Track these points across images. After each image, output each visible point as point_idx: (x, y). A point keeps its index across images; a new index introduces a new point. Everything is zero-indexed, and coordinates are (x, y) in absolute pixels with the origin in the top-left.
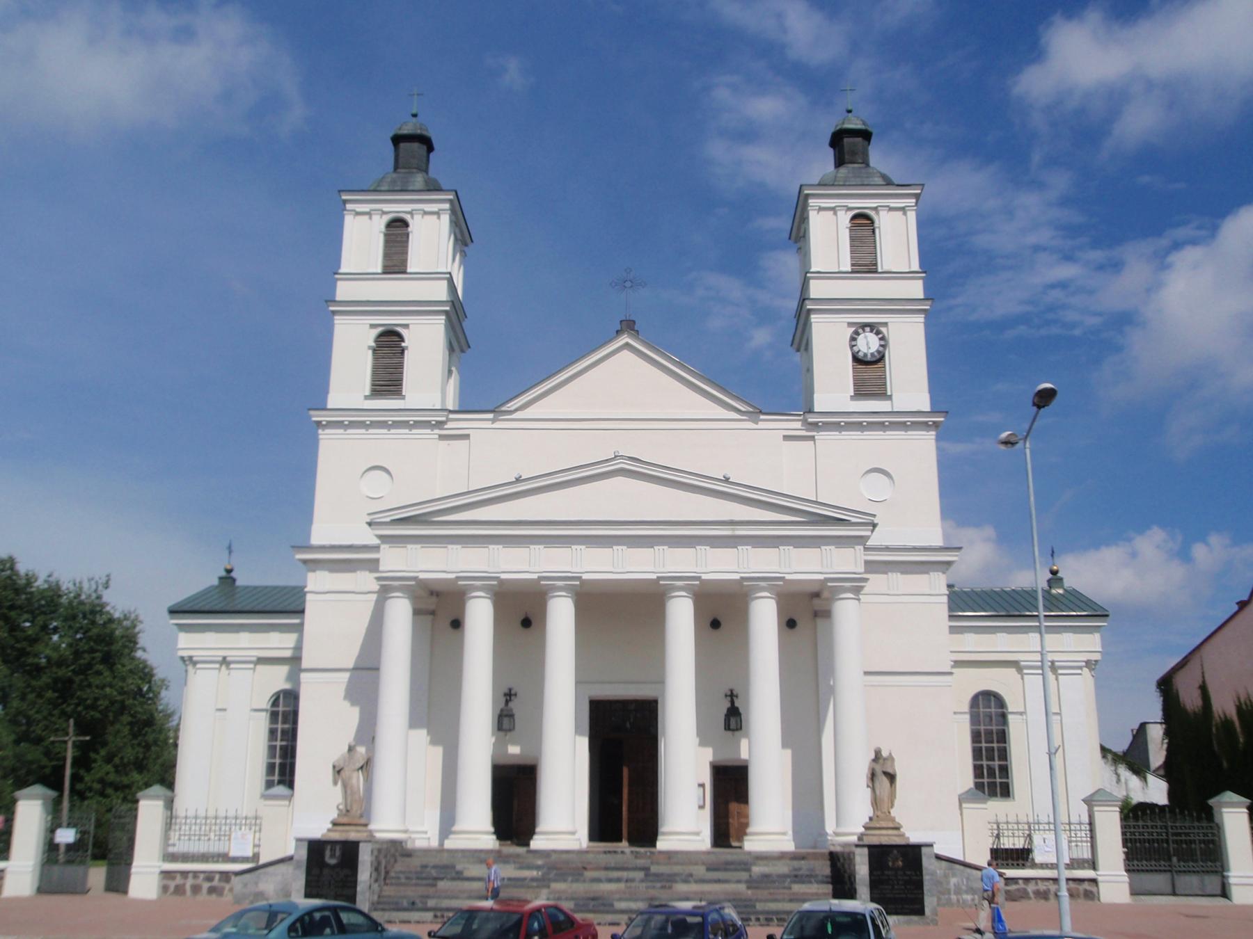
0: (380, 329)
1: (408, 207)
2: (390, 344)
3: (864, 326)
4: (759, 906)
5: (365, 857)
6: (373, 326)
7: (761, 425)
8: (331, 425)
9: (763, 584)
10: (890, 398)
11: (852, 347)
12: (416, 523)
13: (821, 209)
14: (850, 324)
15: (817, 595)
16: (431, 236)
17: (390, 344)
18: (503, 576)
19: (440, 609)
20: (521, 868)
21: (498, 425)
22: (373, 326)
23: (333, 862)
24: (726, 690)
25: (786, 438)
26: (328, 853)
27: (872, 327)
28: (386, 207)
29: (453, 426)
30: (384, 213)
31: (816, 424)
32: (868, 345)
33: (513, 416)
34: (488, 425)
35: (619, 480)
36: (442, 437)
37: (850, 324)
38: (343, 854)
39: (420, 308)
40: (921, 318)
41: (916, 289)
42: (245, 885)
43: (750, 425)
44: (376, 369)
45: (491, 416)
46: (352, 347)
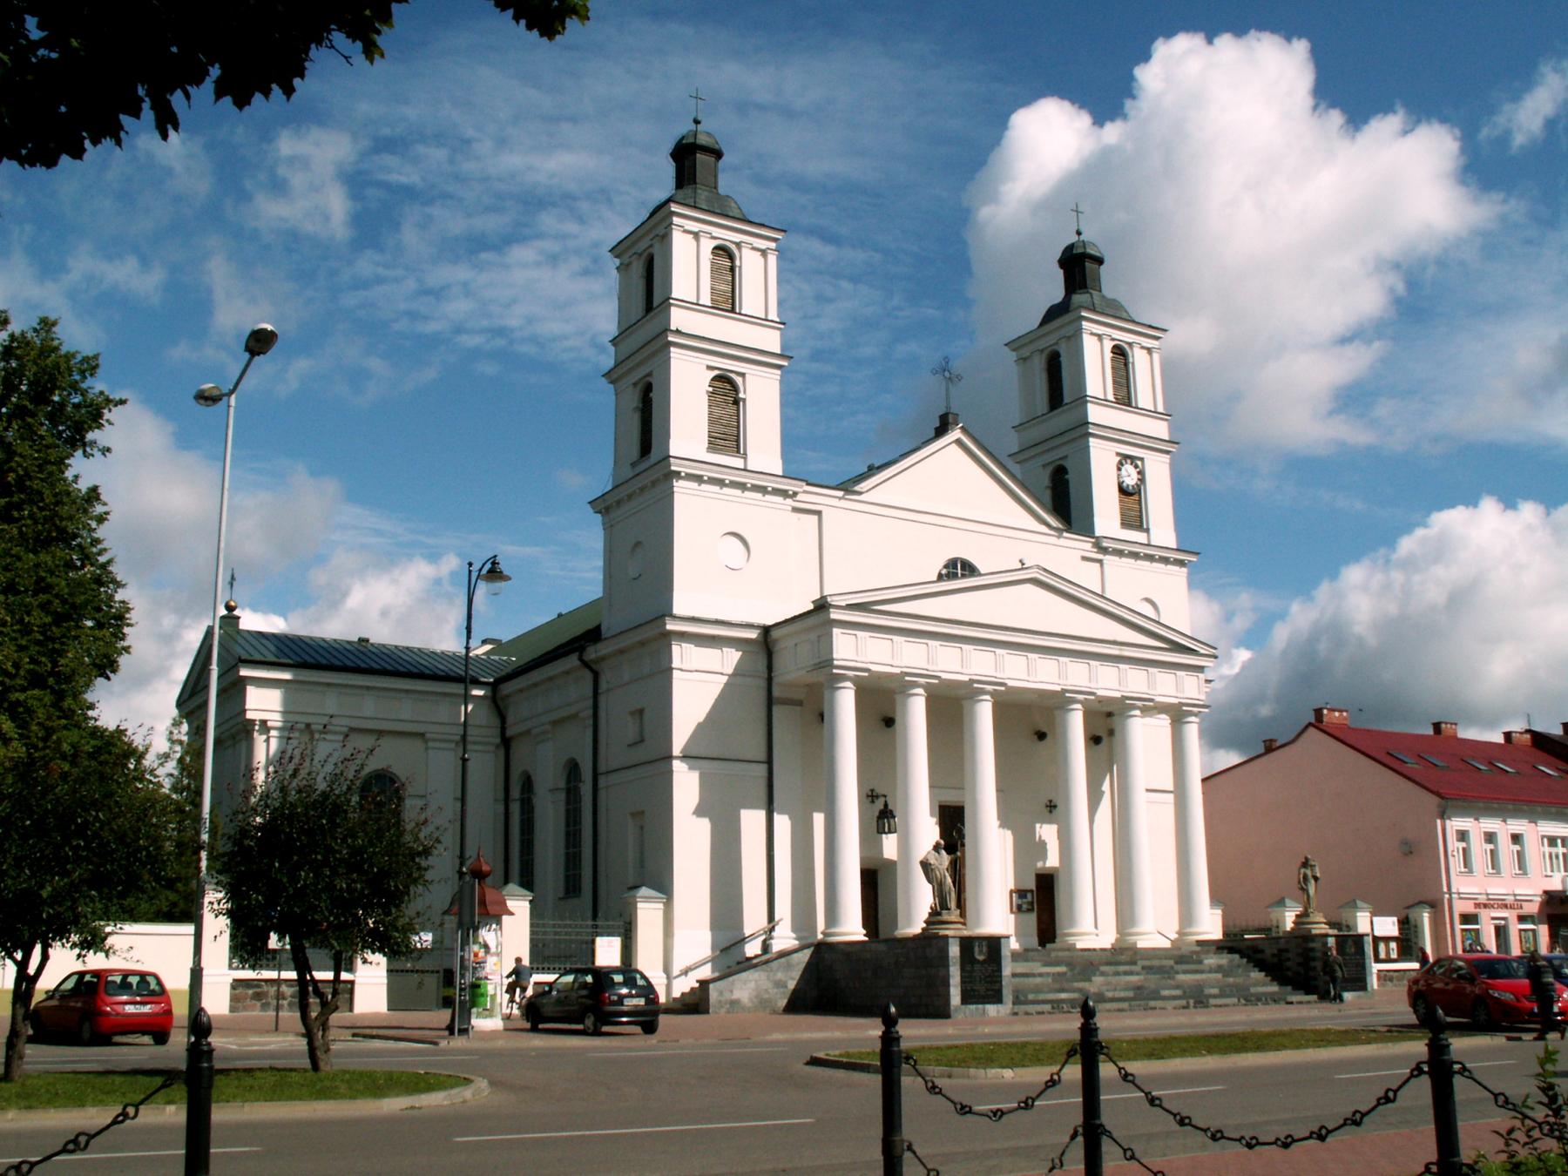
0: (716, 372)
1: (737, 237)
2: (726, 389)
4: (1253, 990)
5: (1005, 953)
6: (710, 368)
7: (1062, 541)
9: (1139, 703)
10: (1147, 531)
11: (1119, 476)
14: (1118, 454)
15: (1110, 715)
16: (758, 275)
17: (726, 389)
18: (944, 676)
20: (1047, 964)
21: (843, 503)
22: (710, 368)
23: (981, 958)
24: (1046, 801)
25: (1084, 558)
26: (976, 949)
27: (1132, 459)
32: (1131, 479)
36: (795, 510)
37: (1118, 454)
38: (989, 947)
39: (756, 357)
42: (721, 993)
43: (1054, 540)
44: (713, 421)
45: (841, 494)
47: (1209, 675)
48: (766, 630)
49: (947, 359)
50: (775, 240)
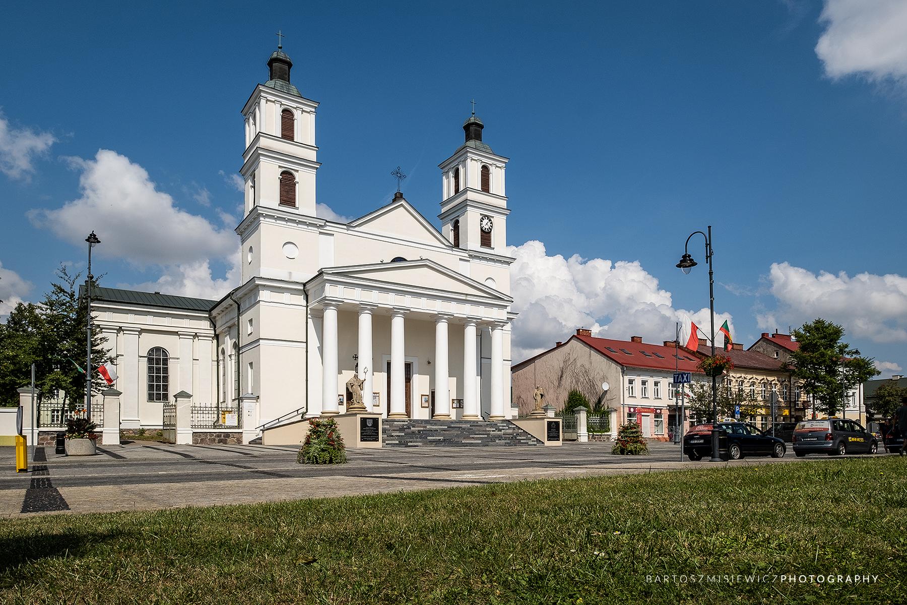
1: (295, 105)
3: (486, 216)
6: (280, 167)
8: (267, 216)
12: (346, 275)
13: (472, 159)
16: (306, 125)
19: (348, 317)
22: (280, 167)
27: (488, 217)
28: (284, 101)
29: (329, 228)
30: (282, 104)
31: (470, 256)
33: (356, 229)
34: (345, 231)
35: (426, 269)
36: (320, 233)
39: (303, 162)
40: (505, 217)
41: (312, 155)
46: (269, 174)
47: (509, 309)
48: (304, 285)
49: (399, 168)
50: (315, 108)
